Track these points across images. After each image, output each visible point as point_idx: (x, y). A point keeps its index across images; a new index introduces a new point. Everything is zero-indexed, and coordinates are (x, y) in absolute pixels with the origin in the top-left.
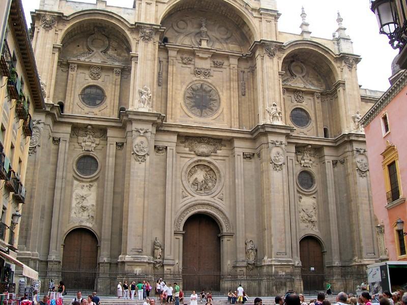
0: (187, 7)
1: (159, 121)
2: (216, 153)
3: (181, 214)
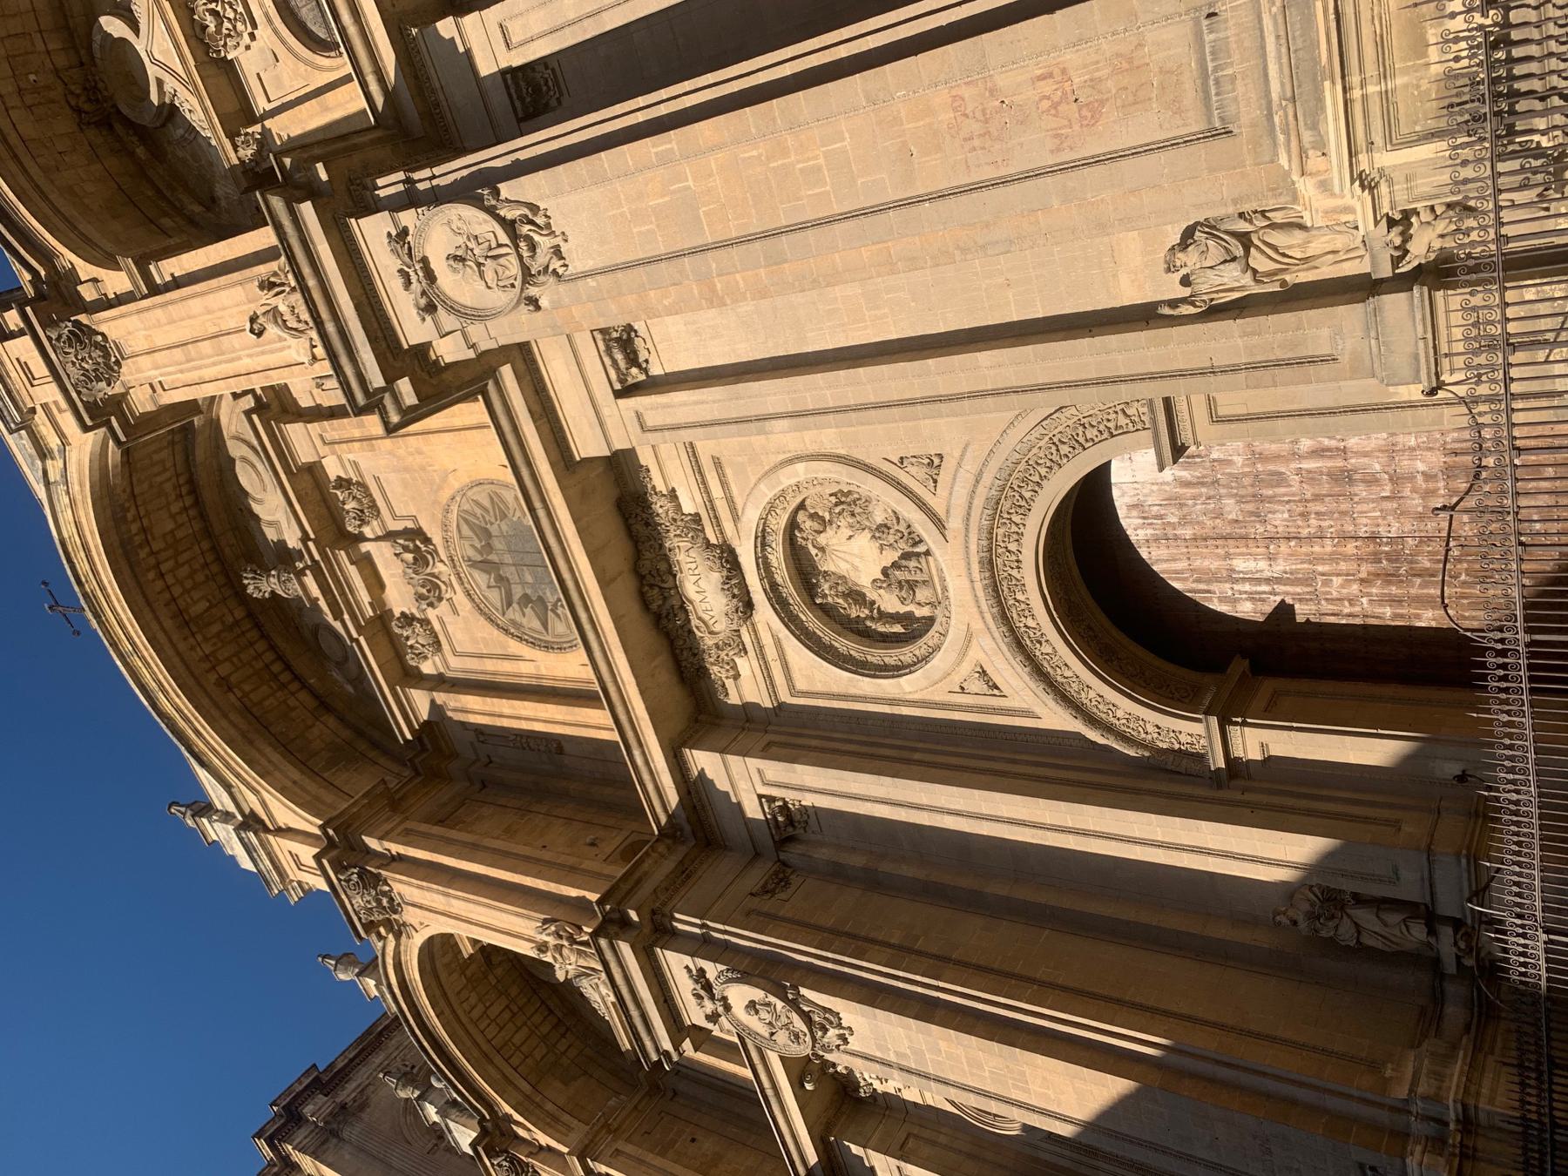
0: (261, 646)
1: (633, 915)
2: (697, 518)
3: (1092, 720)
